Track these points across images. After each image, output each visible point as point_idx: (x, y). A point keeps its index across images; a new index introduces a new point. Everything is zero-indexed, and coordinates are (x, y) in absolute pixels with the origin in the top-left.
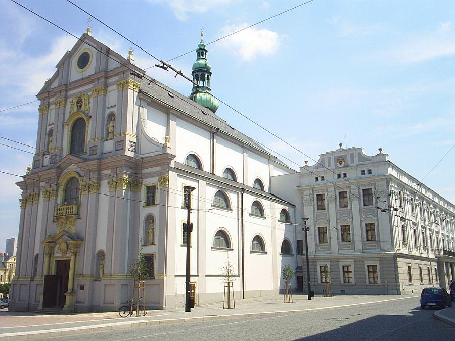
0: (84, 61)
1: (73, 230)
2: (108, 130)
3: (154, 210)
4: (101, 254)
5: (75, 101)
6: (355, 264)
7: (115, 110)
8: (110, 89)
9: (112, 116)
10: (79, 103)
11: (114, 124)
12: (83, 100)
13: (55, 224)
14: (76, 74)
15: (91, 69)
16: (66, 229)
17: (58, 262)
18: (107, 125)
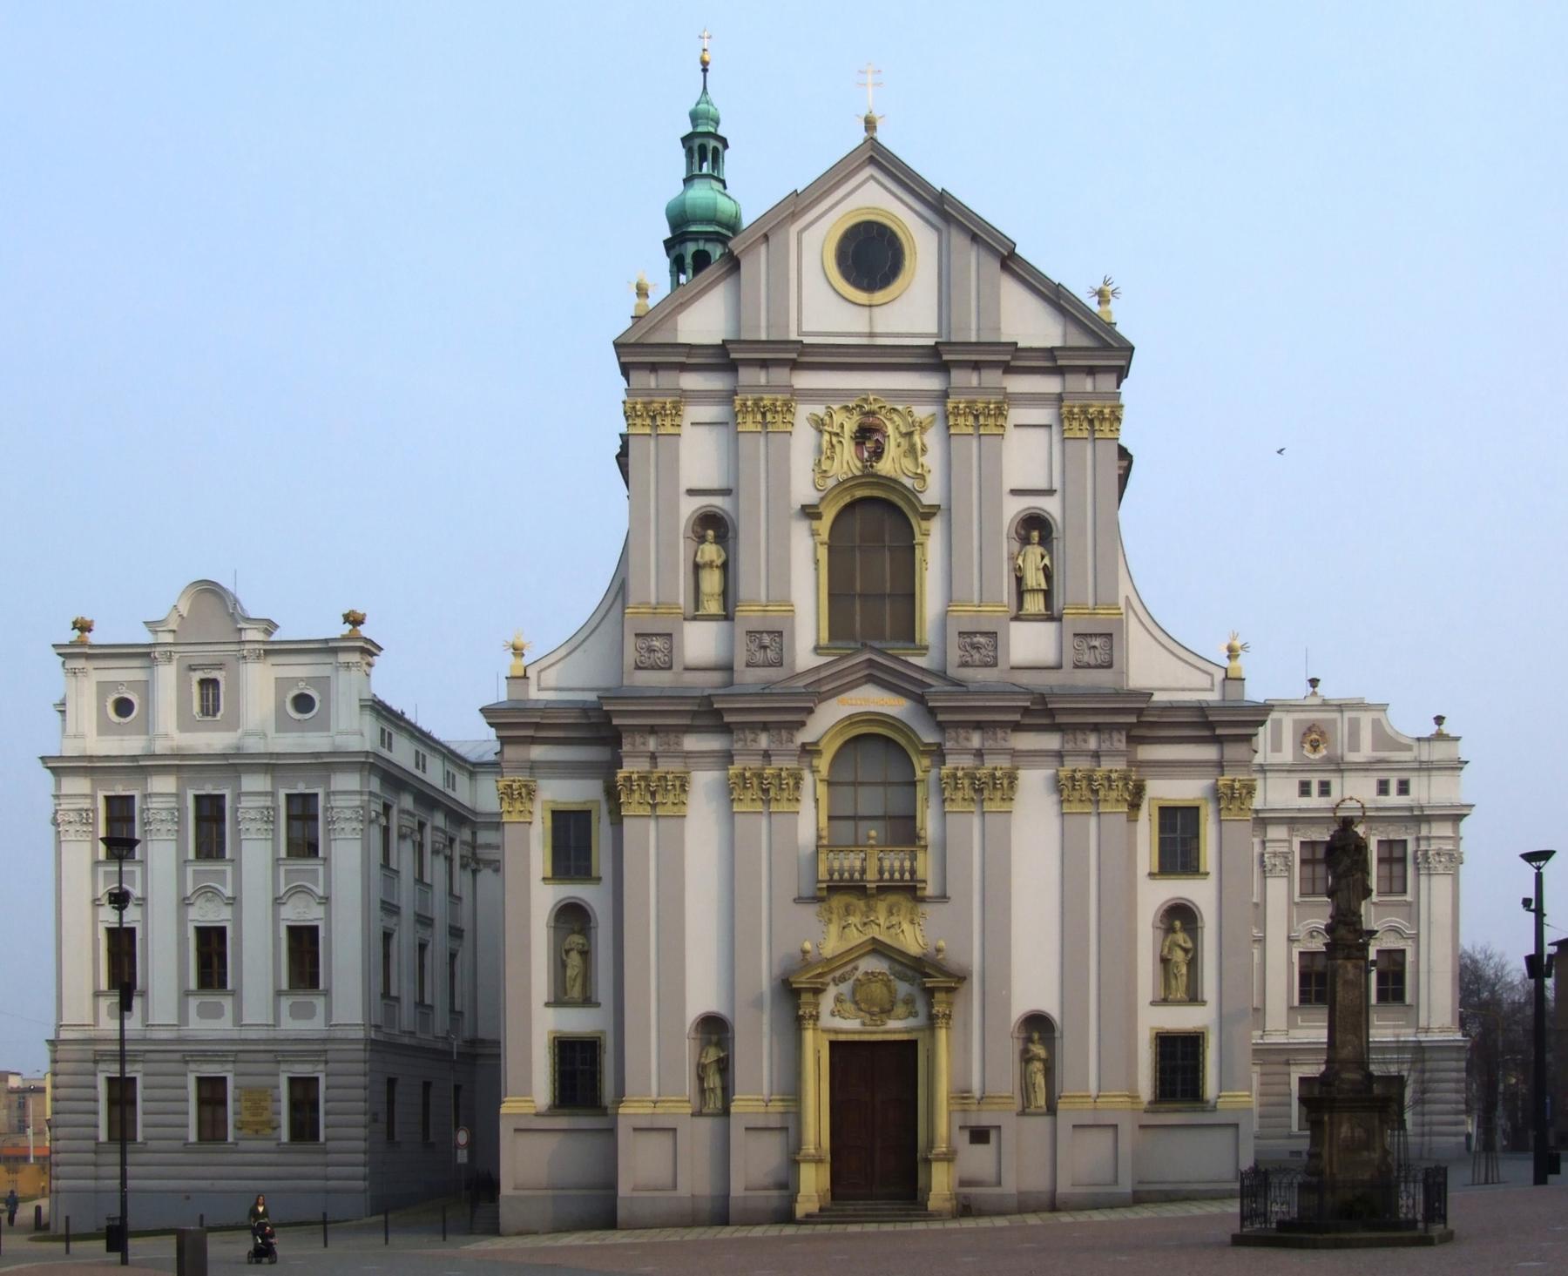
0: (870, 258)
1: (911, 940)
2: (1020, 580)
3: (1199, 892)
4: (1038, 1025)
5: (851, 424)
6: (1263, 1074)
7: (1051, 506)
8: (1016, 415)
9: (1035, 527)
10: (868, 435)
11: (1047, 561)
12: (890, 429)
13: (811, 911)
14: (823, 308)
15: (910, 311)
16: (874, 932)
17: (841, 1050)
18: (1013, 558)
